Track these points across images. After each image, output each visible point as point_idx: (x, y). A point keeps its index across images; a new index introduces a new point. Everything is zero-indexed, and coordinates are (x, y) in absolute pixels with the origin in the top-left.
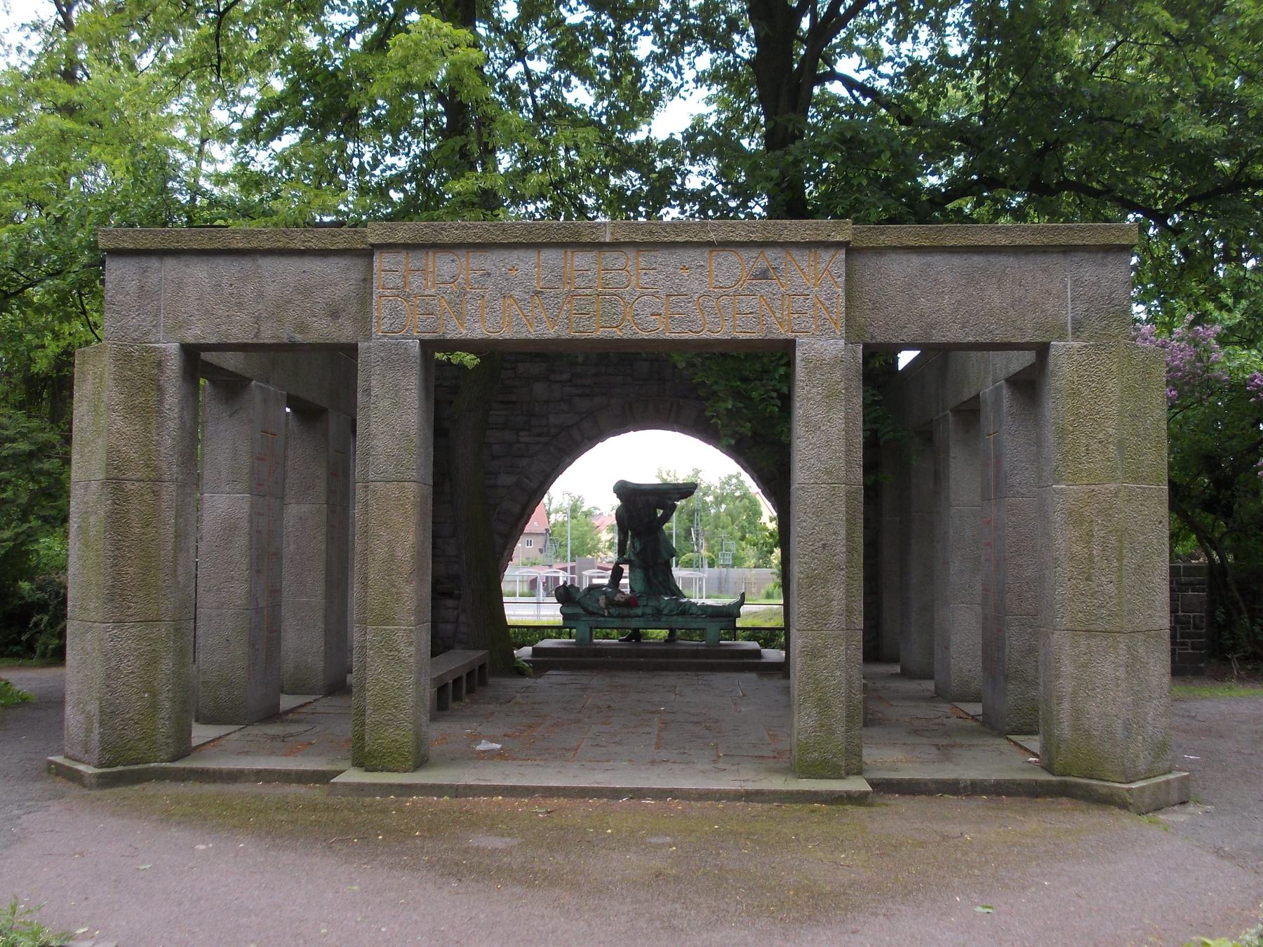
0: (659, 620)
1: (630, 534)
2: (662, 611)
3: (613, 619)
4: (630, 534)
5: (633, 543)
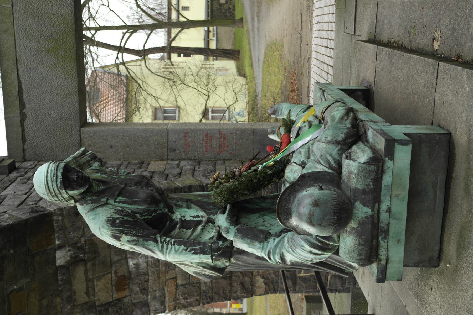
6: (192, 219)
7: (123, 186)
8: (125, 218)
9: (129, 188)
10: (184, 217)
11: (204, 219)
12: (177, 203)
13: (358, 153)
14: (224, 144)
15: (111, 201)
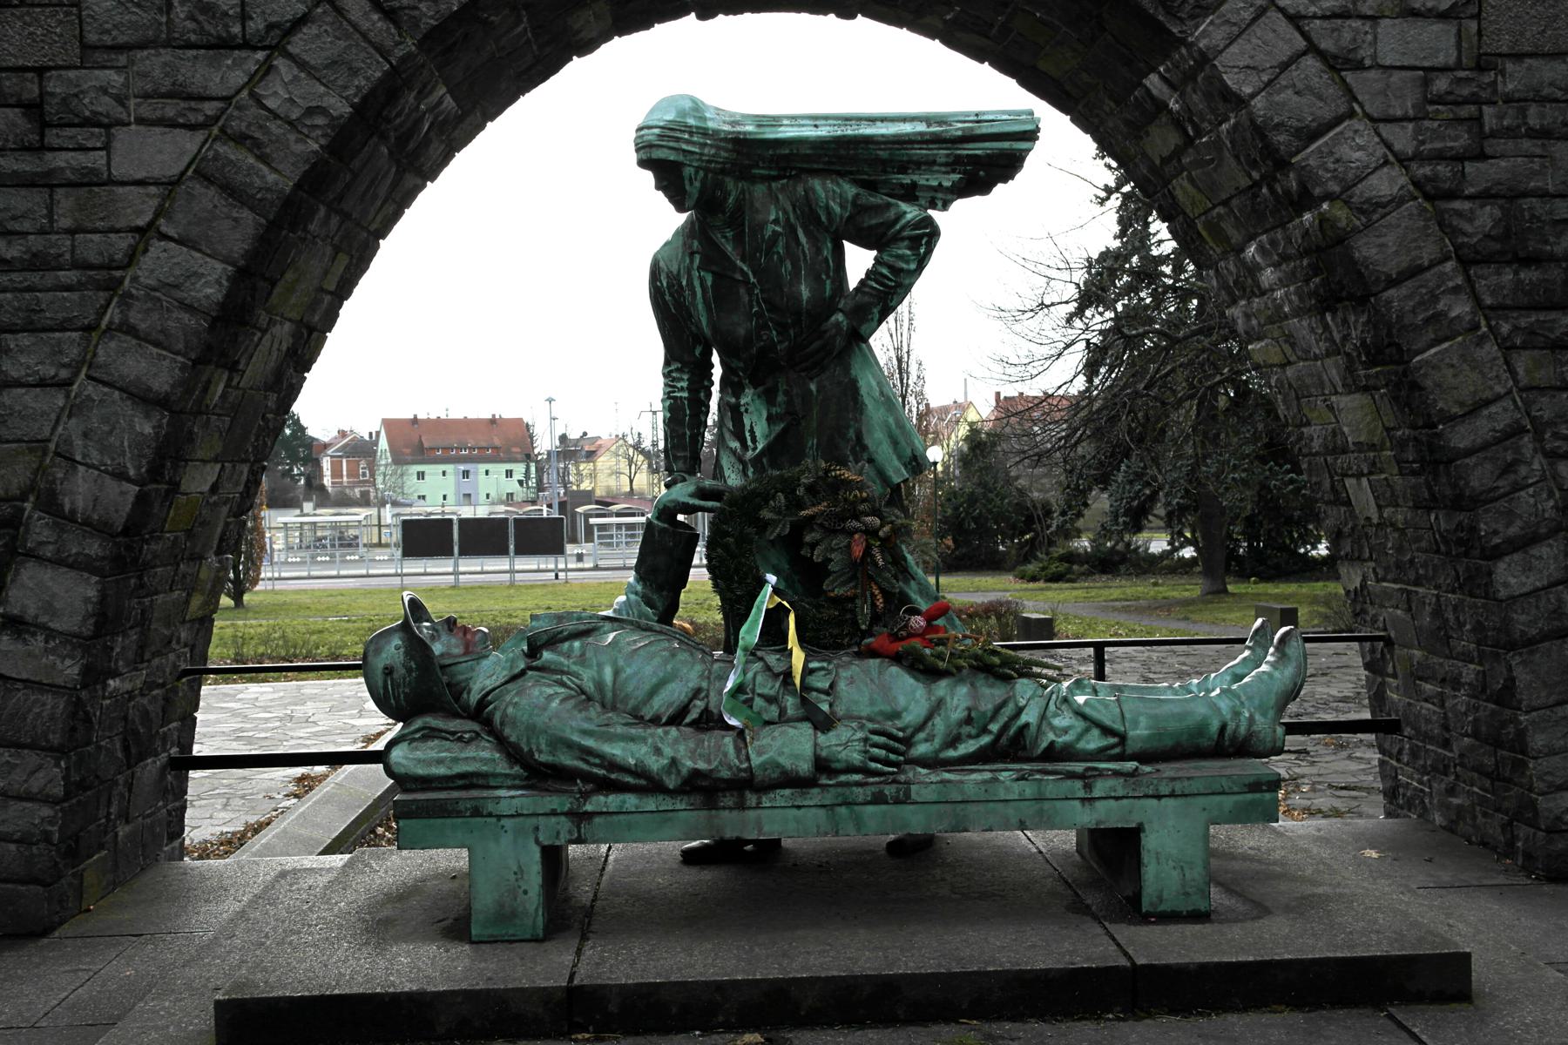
0: (903, 799)
1: (717, 372)
2: (908, 742)
3: (666, 803)
4: (717, 372)
5: (732, 411)
6: (747, 427)
7: (738, 277)
8: (667, 297)
9: (742, 291)
10: (746, 411)
12: (780, 393)
13: (439, 752)
15: (697, 258)
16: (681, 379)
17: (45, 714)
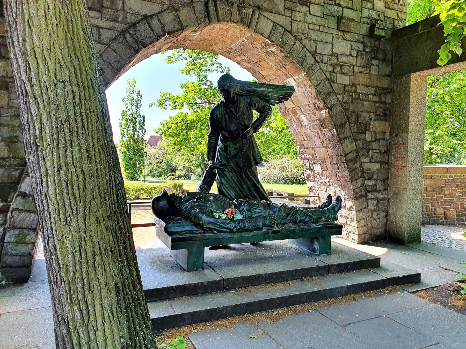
11: (229, 156)
14: (399, 169)
16: (213, 138)
17: (31, 219)
